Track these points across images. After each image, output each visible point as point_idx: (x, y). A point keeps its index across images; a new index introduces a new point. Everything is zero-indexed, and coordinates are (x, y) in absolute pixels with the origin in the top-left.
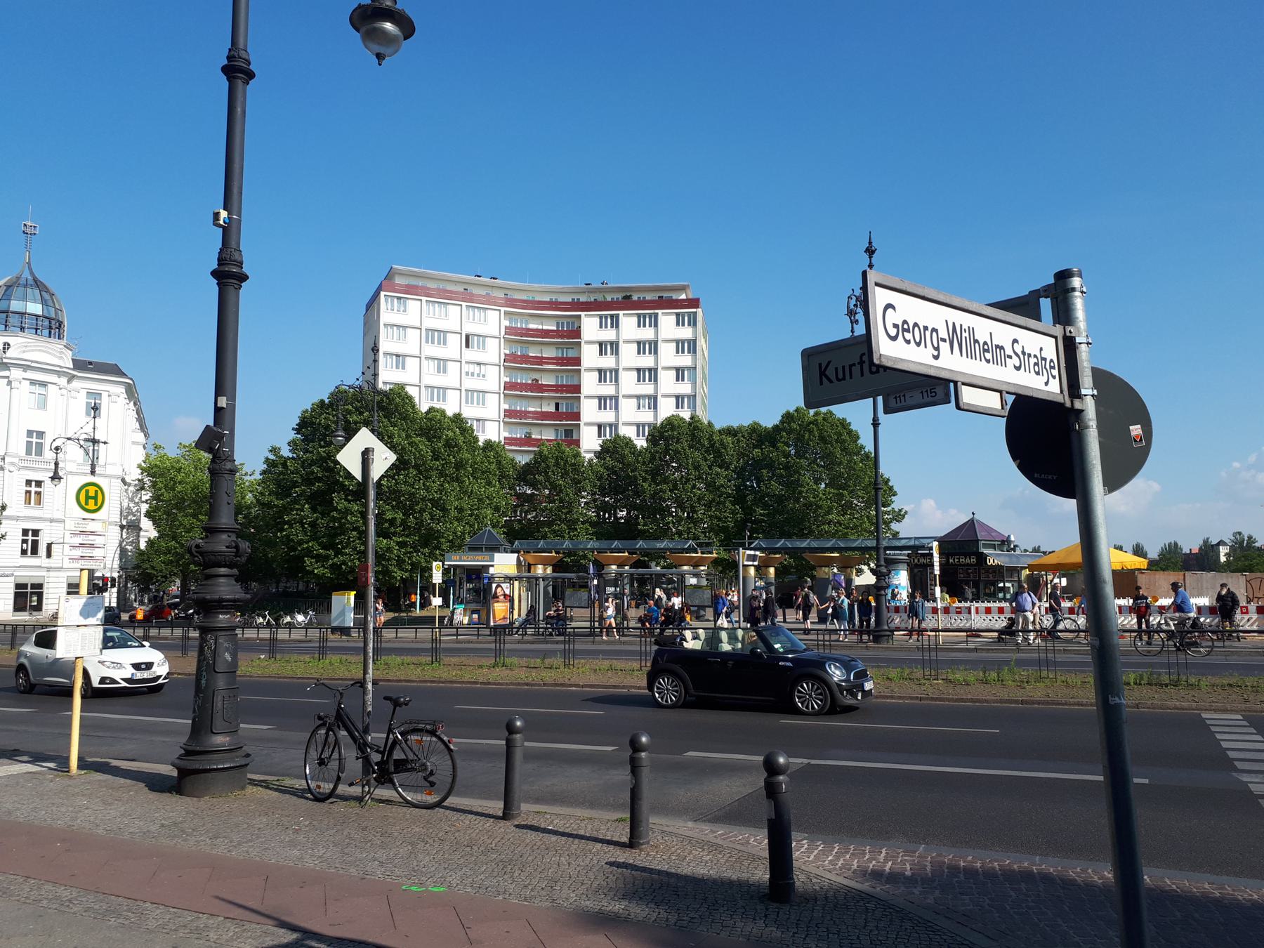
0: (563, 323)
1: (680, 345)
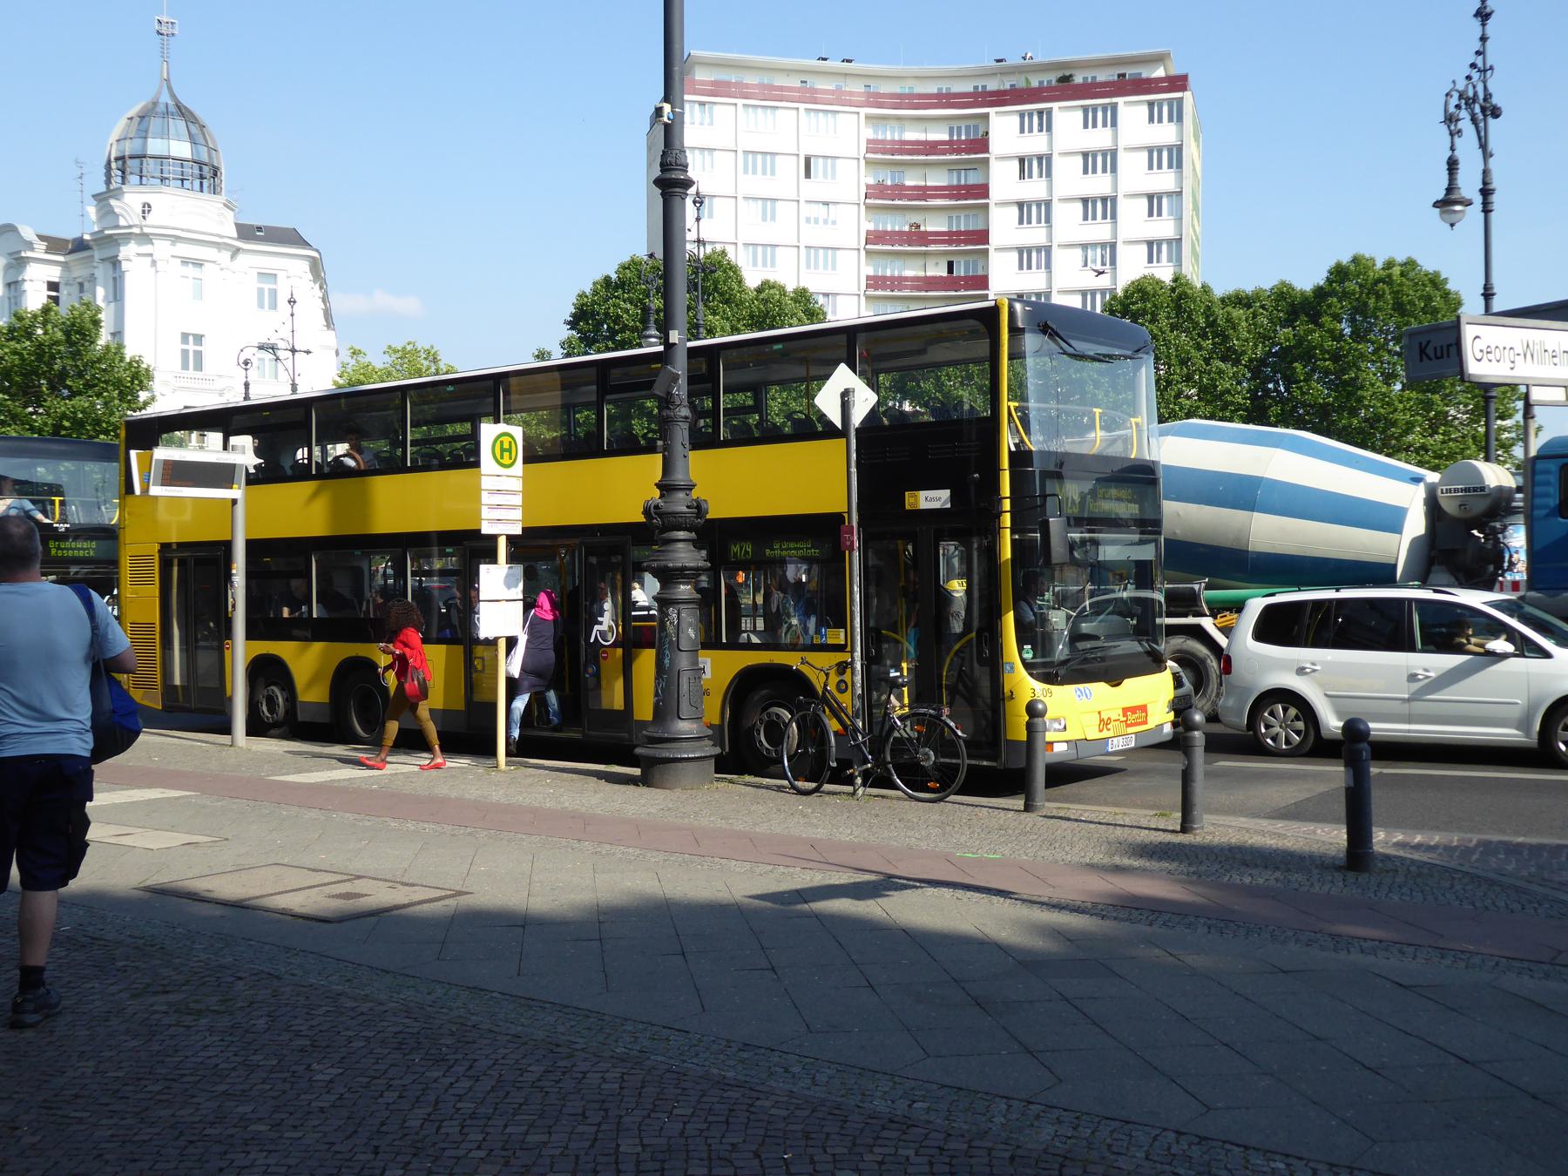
0: (959, 129)
1: (1154, 154)
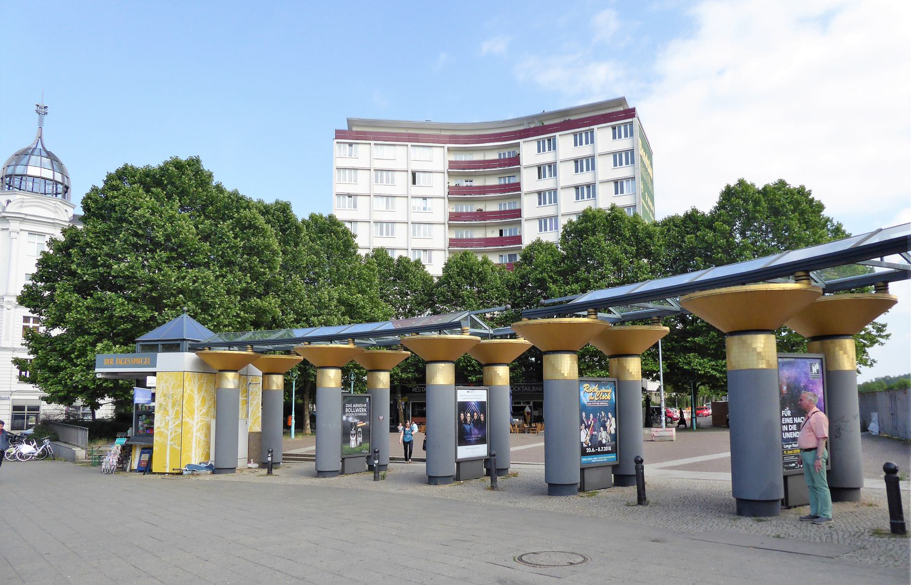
1: (618, 158)
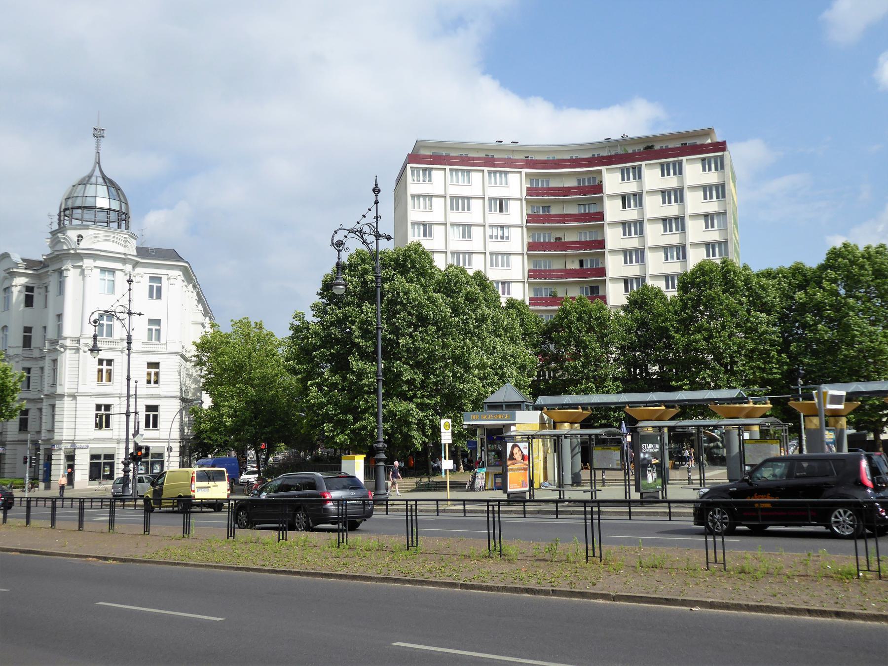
0: (584, 180)
